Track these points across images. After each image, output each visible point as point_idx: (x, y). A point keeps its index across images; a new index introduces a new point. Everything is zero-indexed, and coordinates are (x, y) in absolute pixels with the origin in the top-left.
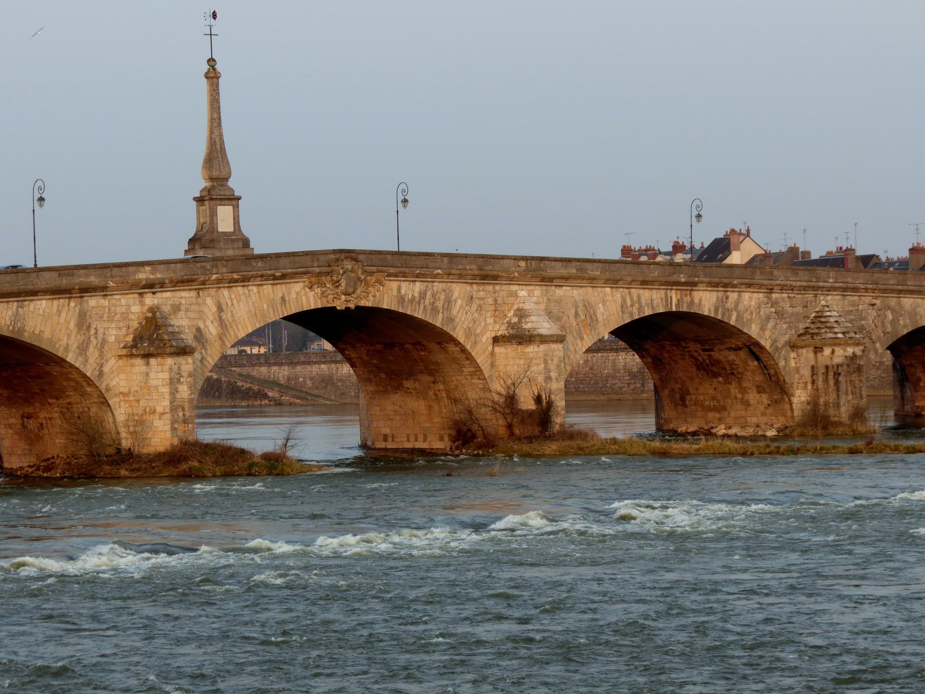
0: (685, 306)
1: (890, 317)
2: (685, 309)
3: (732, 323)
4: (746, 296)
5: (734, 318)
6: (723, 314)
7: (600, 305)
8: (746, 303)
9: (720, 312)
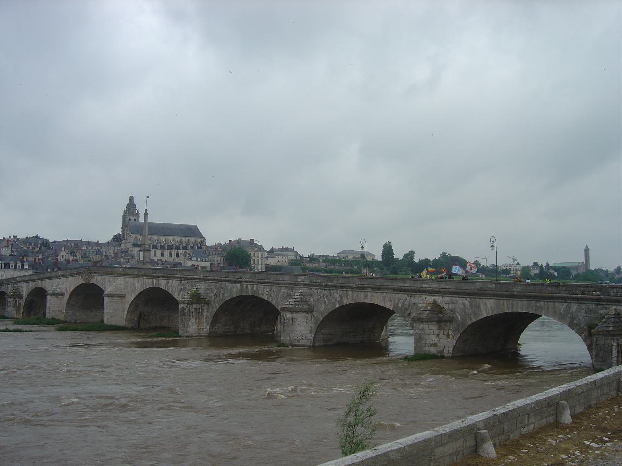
1: (222, 292)
3: (170, 292)
4: (174, 281)
5: (170, 290)
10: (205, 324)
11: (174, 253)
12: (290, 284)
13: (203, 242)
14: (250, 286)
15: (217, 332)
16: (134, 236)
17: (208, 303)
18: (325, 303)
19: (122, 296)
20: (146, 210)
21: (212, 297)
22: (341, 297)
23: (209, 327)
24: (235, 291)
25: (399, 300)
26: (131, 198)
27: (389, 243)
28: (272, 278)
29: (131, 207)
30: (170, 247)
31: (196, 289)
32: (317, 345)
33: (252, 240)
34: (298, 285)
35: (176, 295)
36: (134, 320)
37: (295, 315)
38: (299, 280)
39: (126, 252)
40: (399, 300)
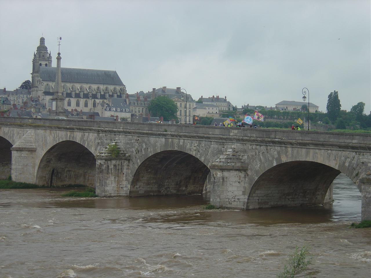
0: (71, 138)
1: (144, 146)
2: (71, 140)
4: (91, 134)
5: (86, 144)
6: (83, 143)
7: (48, 137)
8: (90, 137)
9: (82, 141)
10: (125, 183)
11: (90, 102)
12: (221, 139)
13: (123, 90)
14: (176, 141)
15: (138, 191)
16: (45, 83)
17: (129, 159)
18: (260, 160)
19: (32, 151)
20: (59, 54)
21: (133, 152)
22: (279, 153)
23: (129, 186)
24: (159, 146)
25: (346, 159)
26: (42, 40)
27: (336, 93)
28: (202, 132)
29: (42, 49)
30: (86, 96)
31: (116, 143)
32: (251, 207)
33: (179, 89)
34: (231, 139)
35: (92, 150)
36: (45, 177)
37: (226, 174)
38: (232, 134)
39: (36, 100)
40: (346, 159)
